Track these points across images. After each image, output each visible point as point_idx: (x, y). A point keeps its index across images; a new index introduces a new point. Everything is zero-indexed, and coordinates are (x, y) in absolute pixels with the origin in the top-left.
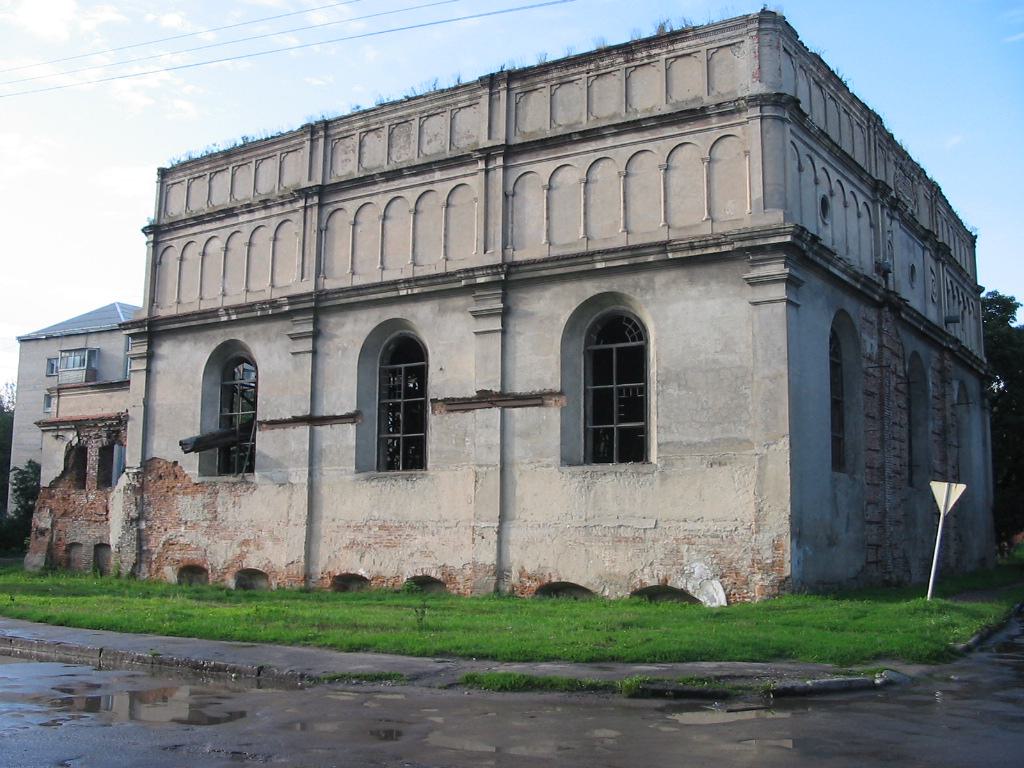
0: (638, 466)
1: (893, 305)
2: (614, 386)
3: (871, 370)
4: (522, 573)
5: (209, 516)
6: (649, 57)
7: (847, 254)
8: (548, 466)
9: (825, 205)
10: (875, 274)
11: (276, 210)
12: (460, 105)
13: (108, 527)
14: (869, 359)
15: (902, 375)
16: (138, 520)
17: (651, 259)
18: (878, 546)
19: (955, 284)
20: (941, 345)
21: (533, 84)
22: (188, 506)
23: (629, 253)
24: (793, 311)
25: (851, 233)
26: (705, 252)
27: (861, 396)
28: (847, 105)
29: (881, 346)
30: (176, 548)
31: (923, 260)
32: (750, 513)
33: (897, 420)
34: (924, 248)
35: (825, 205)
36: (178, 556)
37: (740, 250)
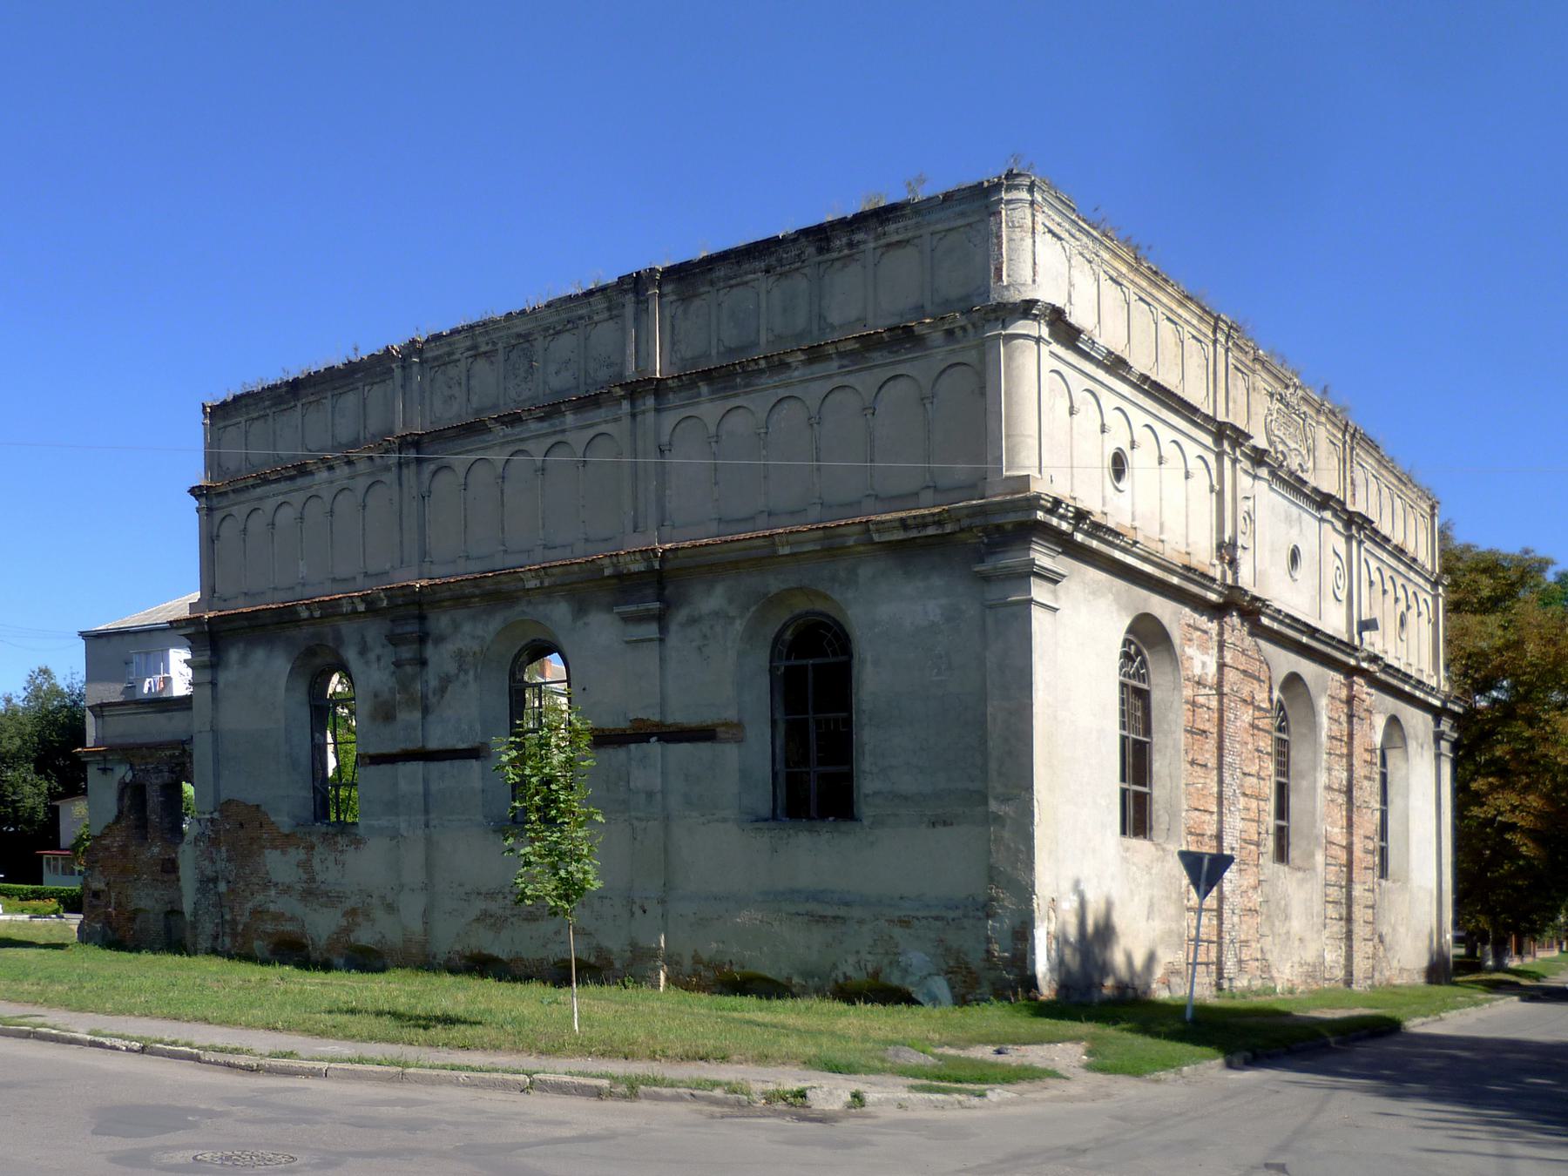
0: (845, 826)
1: (1238, 606)
2: (811, 716)
3: (1201, 700)
5: (304, 877)
7: (1161, 532)
8: (724, 820)
13: (179, 889)
15: (1266, 705)
16: (215, 880)
19: (1387, 573)
20: (1346, 664)
22: (280, 865)
26: (923, 534)
29: (1222, 666)
31: (1322, 539)
33: (1254, 769)
34: (1321, 520)
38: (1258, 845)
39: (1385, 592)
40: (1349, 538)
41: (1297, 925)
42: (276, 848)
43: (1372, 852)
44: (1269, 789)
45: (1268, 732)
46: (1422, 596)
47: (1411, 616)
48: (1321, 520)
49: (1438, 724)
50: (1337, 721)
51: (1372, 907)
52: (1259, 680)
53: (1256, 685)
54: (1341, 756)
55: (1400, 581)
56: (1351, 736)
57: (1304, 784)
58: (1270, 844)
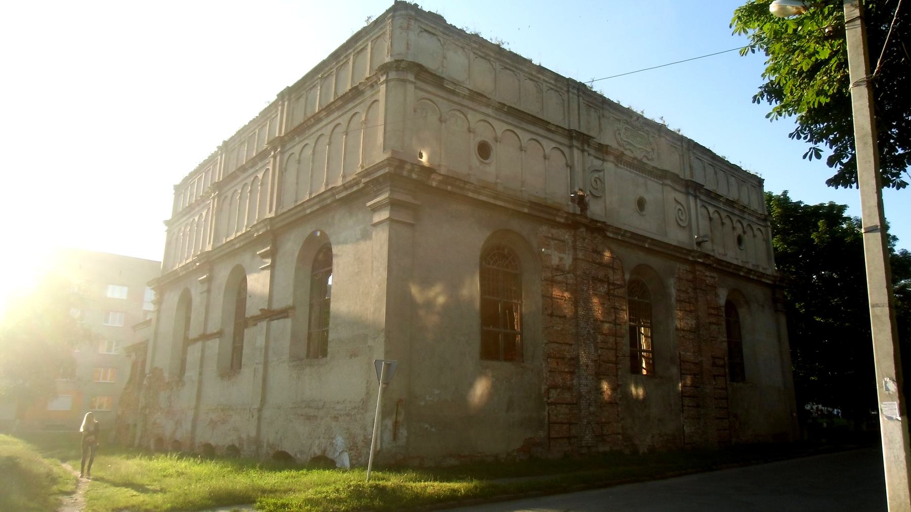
3: (559, 278)
4: (268, 442)
6: (346, 57)
9: (484, 150)
10: (570, 203)
14: (558, 269)
17: (329, 201)
18: (570, 424)
19: (724, 214)
20: (688, 260)
23: (317, 200)
28: (532, 75)
29: (575, 259)
34: (663, 184)
35: (484, 150)
37: (366, 184)
38: (616, 363)
40: (688, 194)
43: (723, 366)
46: (755, 227)
47: (745, 237)
50: (686, 292)
52: (613, 269)
53: (611, 272)
54: (691, 312)
55: (735, 219)
56: (697, 300)
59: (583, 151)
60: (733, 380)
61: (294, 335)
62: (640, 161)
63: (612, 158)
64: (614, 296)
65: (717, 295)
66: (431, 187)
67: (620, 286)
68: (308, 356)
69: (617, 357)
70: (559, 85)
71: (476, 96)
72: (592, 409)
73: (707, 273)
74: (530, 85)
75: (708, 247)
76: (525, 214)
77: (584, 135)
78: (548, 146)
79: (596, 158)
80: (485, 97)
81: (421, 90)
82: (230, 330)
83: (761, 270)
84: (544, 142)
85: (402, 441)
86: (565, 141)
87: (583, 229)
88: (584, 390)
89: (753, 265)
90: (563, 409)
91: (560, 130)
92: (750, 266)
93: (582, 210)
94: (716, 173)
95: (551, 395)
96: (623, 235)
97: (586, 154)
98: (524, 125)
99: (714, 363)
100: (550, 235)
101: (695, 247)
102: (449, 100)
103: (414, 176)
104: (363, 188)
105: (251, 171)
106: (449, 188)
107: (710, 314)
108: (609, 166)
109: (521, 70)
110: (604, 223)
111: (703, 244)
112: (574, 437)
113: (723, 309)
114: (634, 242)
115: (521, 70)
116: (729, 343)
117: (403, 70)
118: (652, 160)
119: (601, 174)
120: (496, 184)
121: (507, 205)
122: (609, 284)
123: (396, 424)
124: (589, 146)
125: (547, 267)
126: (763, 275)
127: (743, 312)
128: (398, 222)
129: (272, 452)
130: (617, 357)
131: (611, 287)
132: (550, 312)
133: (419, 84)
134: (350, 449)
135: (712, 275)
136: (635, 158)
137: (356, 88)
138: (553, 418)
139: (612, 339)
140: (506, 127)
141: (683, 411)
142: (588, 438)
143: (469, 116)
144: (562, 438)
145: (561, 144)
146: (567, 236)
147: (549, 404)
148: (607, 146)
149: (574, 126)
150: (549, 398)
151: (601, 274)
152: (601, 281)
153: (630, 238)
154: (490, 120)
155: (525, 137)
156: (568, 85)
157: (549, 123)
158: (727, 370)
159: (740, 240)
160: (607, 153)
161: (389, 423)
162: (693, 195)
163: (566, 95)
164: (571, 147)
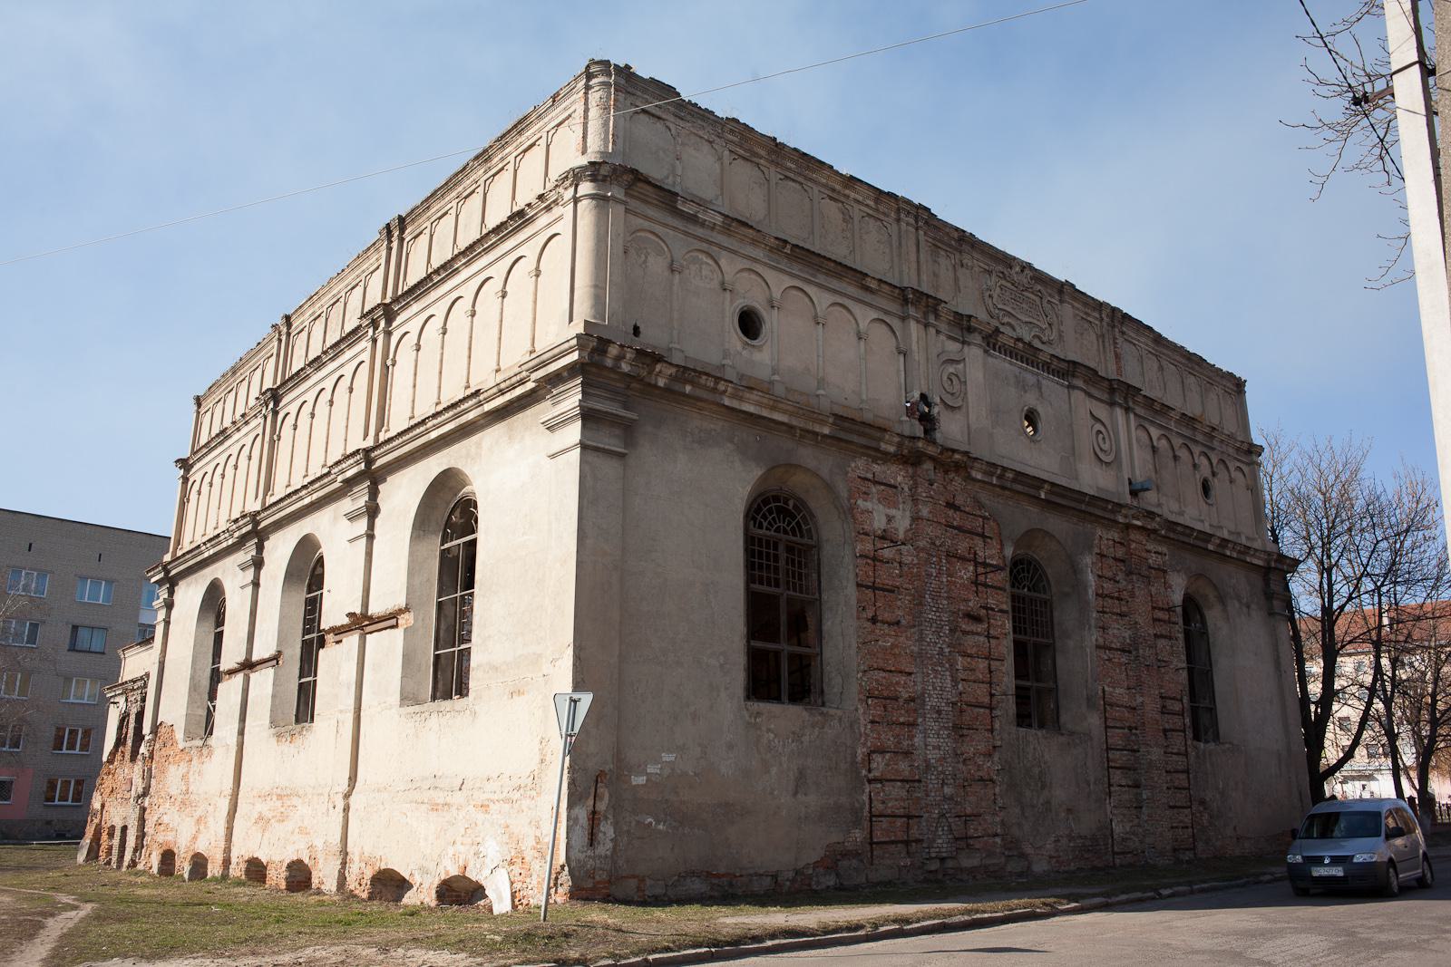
3: (887, 553)
6: (502, 159)
9: (749, 324)
11: (253, 424)
12: (371, 269)
17: (471, 416)
18: (909, 817)
19: (1177, 442)
21: (420, 226)
24: (609, 468)
25: (839, 354)
27: (851, 590)
28: (834, 190)
29: (916, 519)
30: (162, 828)
32: (534, 765)
35: (749, 324)
36: (160, 838)
38: (991, 708)
39: (1176, 458)
41: (1059, 794)
42: (175, 763)
44: (1006, 647)
45: (1005, 590)
46: (1232, 466)
47: (1216, 484)
48: (1071, 387)
49: (1267, 582)
50: (1113, 580)
51: (1187, 772)
52: (983, 536)
53: (979, 541)
54: (1122, 615)
55: (1196, 450)
56: (1132, 595)
57: (1071, 643)
58: (1010, 706)
59: (926, 326)
60: (1197, 737)
61: (408, 659)
62: (1030, 345)
63: (977, 339)
64: (985, 585)
65: (1167, 586)
66: (656, 386)
67: (998, 568)
68: (434, 698)
69: (992, 695)
70: (881, 208)
71: (735, 224)
72: (948, 790)
73: (1150, 547)
74: (832, 209)
75: (1150, 498)
76: (825, 436)
77: (928, 296)
78: (865, 316)
79: (950, 338)
80: (751, 227)
81: (636, 214)
82: (294, 652)
83: (1244, 541)
84: (857, 309)
85: (604, 848)
86: (894, 307)
87: (928, 465)
88: (933, 755)
89: (1230, 533)
90: (897, 791)
91: (886, 288)
92: (1226, 535)
93: (926, 432)
94: (1161, 368)
95: (874, 765)
96: (1000, 477)
97: (932, 331)
98: (821, 279)
99: (1164, 707)
100: (870, 476)
101: (1128, 499)
102: (686, 233)
103: (625, 367)
104: (533, 391)
105: (331, 366)
106: (688, 388)
107: (1155, 620)
108: (974, 354)
109: (815, 181)
110: (966, 453)
111: (1141, 494)
112: (918, 841)
113: (1179, 610)
114: (1019, 487)
115: (815, 181)
116: (1191, 671)
117: (604, 180)
118: (1050, 343)
119: (960, 366)
120: (771, 383)
121: (795, 422)
122: (976, 564)
123: (594, 812)
124: (937, 316)
125: (866, 534)
126: (1247, 549)
127: (1213, 616)
128: (597, 449)
129: (369, 874)
130: (992, 695)
131: (980, 570)
132: (870, 615)
133: (634, 204)
134: (512, 863)
135: (1160, 549)
136: (1019, 340)
137: (521, 213)
138: (878, 807)
139: (982, 664)
140: (789, 282)
141: (1110, 794)
142: (942, 843)
143: (723, 262)
144: (892, 842)
145: (887, 312)
146: (897, 474)
147: (870, 781)
148: (970, 317)
149: (909, 280)
150: (870, 771)
151: (962, 547)
152: (962, 559)
153: (1014, 480)
154: (759, 268)
155: (823, 299)
156: (898, 211)
157: (866, 275)
158: (1187, 720)
159: (1206, 489)
160: (970, 330)
161: (582, 814)
162: (1120, 405)
163: (895, 226)
164: (904, 319)
